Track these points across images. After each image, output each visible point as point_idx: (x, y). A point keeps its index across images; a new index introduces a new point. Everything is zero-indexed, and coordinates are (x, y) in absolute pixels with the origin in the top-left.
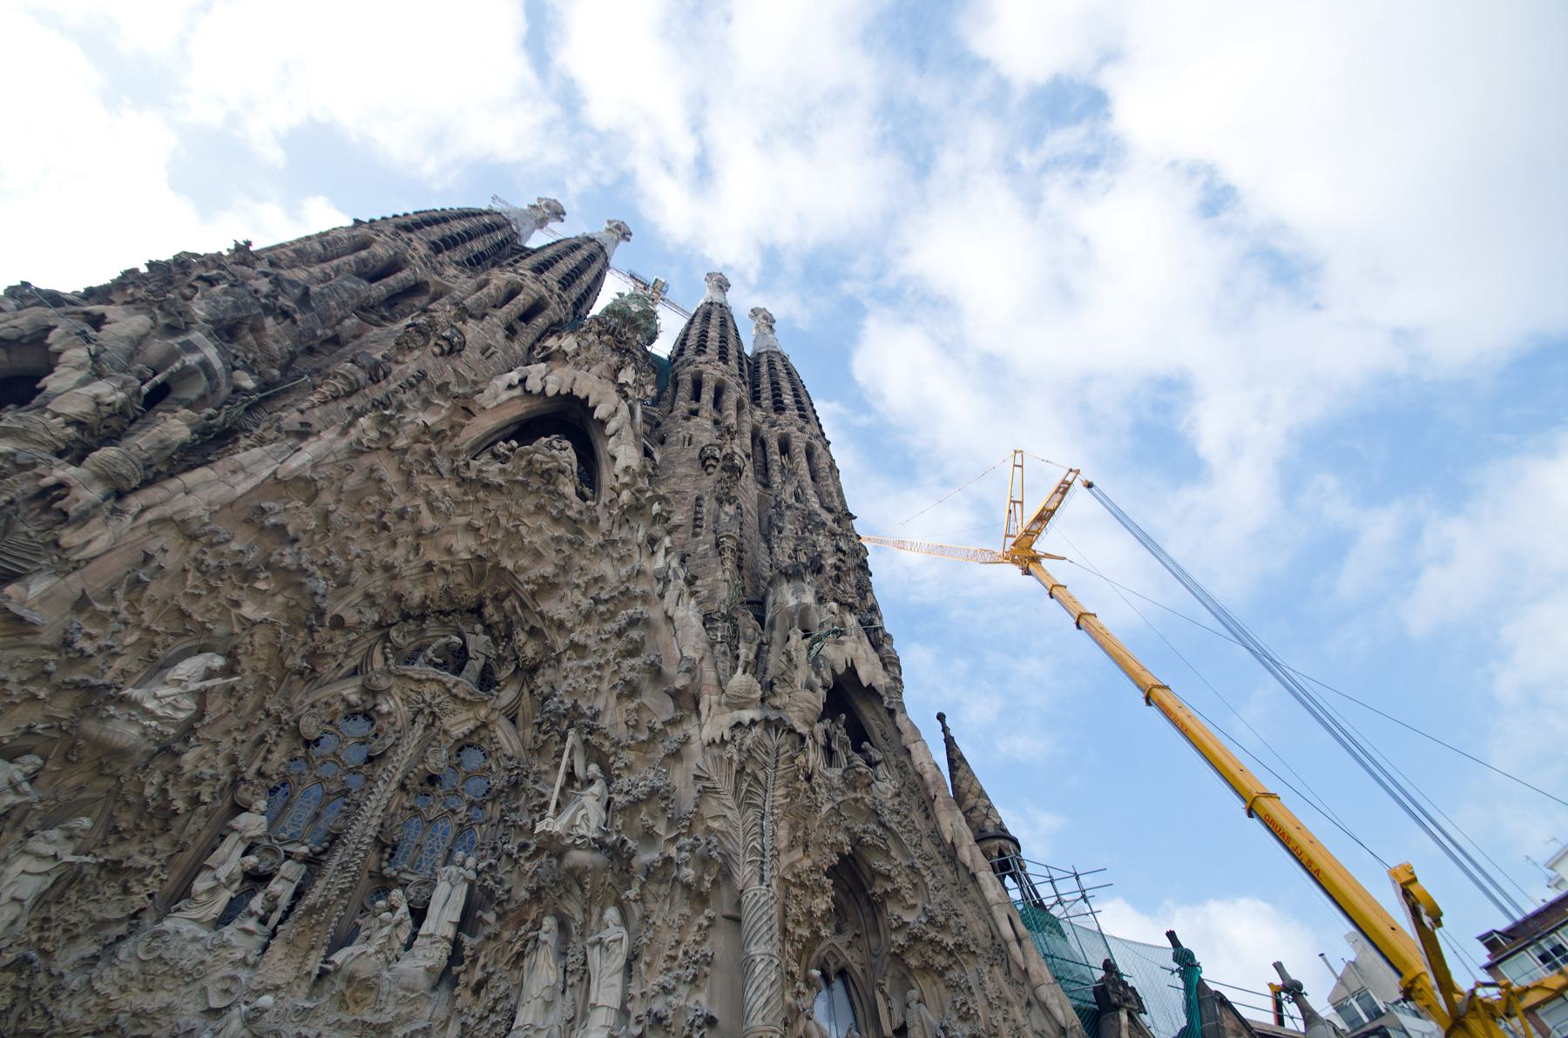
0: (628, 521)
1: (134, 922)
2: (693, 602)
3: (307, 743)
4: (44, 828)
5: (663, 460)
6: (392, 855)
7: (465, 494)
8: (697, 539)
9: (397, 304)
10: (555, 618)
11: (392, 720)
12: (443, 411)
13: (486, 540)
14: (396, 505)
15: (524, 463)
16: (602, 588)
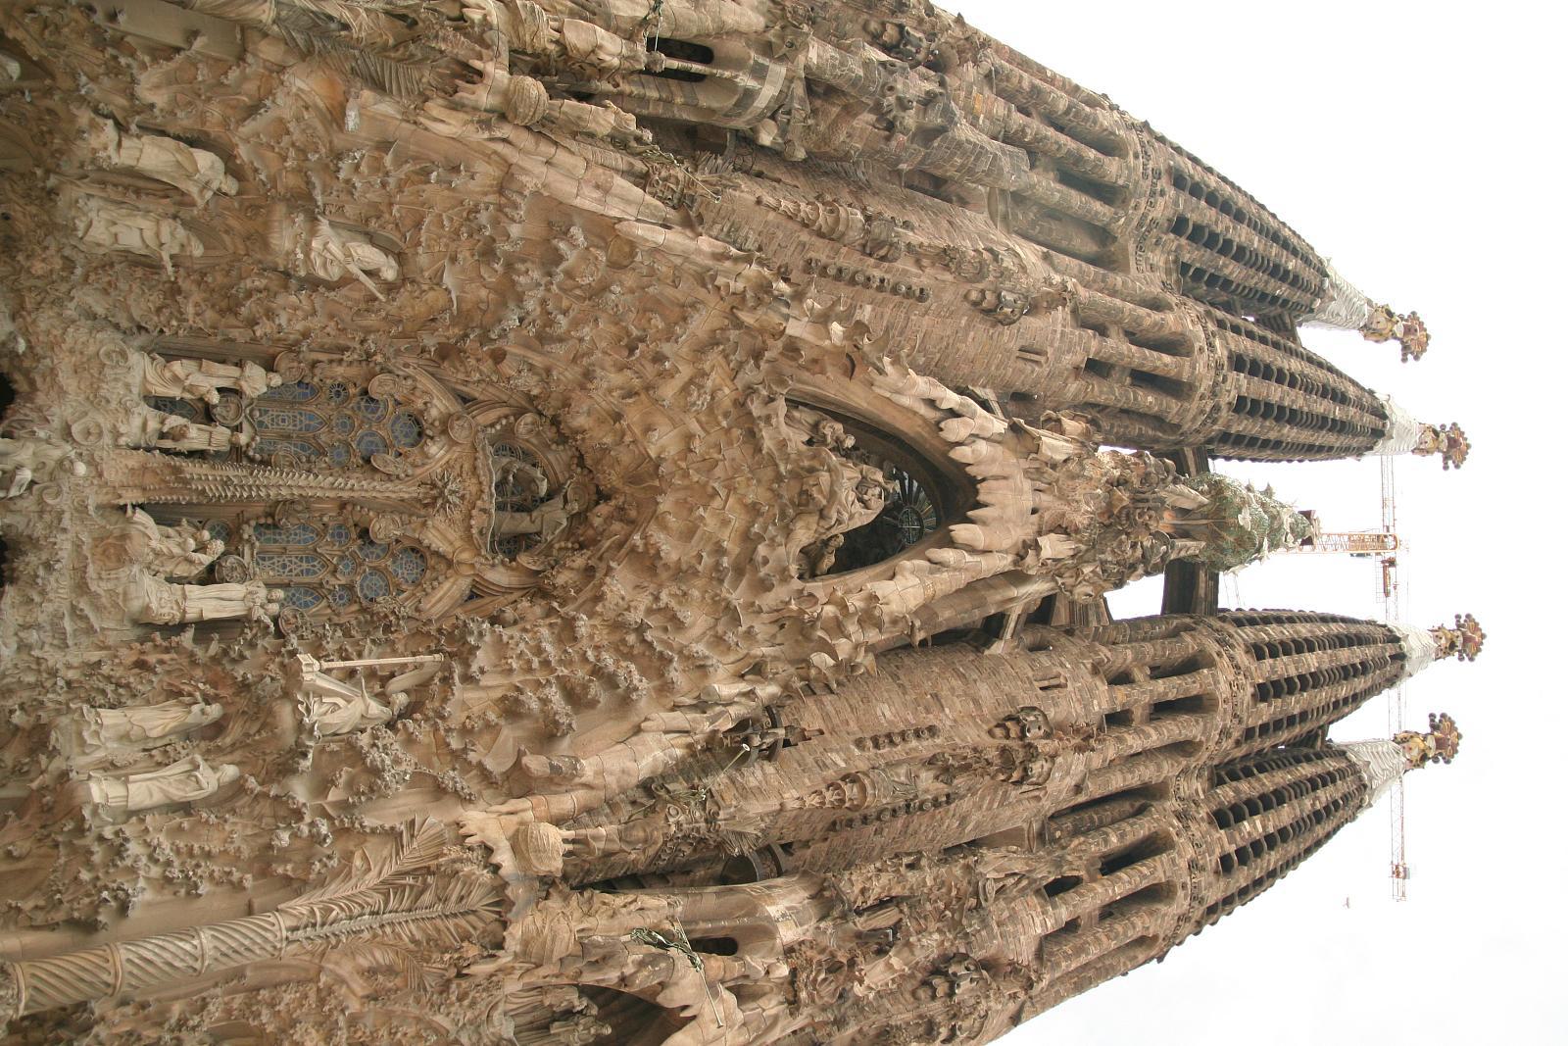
0: (782, 627)
1: (135, 330)
2: (679, 752)
3: (365, 392)
4: (184, 224)
5: (998, 659)
6: (268, 526)
7: (726, 415)
8: (853, 747)
9: (1060, 220)
10: (604, 588)
11: (419, 461)
12: (827, 342)
13: (683, 465)
14: (666, 348)
15: (806, 463)
16: (666, 630)
